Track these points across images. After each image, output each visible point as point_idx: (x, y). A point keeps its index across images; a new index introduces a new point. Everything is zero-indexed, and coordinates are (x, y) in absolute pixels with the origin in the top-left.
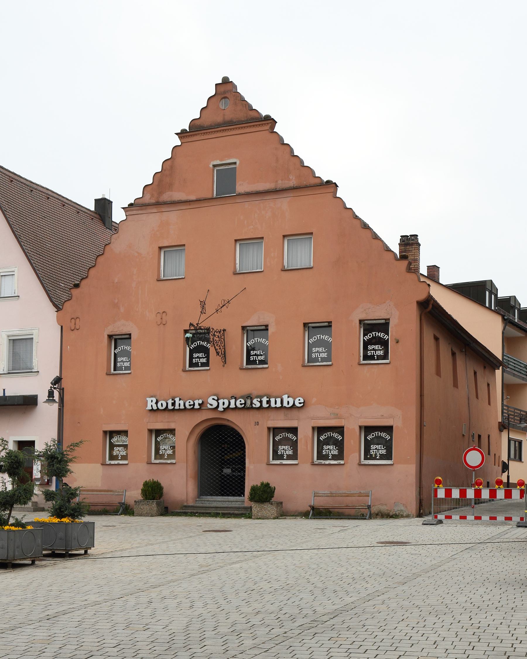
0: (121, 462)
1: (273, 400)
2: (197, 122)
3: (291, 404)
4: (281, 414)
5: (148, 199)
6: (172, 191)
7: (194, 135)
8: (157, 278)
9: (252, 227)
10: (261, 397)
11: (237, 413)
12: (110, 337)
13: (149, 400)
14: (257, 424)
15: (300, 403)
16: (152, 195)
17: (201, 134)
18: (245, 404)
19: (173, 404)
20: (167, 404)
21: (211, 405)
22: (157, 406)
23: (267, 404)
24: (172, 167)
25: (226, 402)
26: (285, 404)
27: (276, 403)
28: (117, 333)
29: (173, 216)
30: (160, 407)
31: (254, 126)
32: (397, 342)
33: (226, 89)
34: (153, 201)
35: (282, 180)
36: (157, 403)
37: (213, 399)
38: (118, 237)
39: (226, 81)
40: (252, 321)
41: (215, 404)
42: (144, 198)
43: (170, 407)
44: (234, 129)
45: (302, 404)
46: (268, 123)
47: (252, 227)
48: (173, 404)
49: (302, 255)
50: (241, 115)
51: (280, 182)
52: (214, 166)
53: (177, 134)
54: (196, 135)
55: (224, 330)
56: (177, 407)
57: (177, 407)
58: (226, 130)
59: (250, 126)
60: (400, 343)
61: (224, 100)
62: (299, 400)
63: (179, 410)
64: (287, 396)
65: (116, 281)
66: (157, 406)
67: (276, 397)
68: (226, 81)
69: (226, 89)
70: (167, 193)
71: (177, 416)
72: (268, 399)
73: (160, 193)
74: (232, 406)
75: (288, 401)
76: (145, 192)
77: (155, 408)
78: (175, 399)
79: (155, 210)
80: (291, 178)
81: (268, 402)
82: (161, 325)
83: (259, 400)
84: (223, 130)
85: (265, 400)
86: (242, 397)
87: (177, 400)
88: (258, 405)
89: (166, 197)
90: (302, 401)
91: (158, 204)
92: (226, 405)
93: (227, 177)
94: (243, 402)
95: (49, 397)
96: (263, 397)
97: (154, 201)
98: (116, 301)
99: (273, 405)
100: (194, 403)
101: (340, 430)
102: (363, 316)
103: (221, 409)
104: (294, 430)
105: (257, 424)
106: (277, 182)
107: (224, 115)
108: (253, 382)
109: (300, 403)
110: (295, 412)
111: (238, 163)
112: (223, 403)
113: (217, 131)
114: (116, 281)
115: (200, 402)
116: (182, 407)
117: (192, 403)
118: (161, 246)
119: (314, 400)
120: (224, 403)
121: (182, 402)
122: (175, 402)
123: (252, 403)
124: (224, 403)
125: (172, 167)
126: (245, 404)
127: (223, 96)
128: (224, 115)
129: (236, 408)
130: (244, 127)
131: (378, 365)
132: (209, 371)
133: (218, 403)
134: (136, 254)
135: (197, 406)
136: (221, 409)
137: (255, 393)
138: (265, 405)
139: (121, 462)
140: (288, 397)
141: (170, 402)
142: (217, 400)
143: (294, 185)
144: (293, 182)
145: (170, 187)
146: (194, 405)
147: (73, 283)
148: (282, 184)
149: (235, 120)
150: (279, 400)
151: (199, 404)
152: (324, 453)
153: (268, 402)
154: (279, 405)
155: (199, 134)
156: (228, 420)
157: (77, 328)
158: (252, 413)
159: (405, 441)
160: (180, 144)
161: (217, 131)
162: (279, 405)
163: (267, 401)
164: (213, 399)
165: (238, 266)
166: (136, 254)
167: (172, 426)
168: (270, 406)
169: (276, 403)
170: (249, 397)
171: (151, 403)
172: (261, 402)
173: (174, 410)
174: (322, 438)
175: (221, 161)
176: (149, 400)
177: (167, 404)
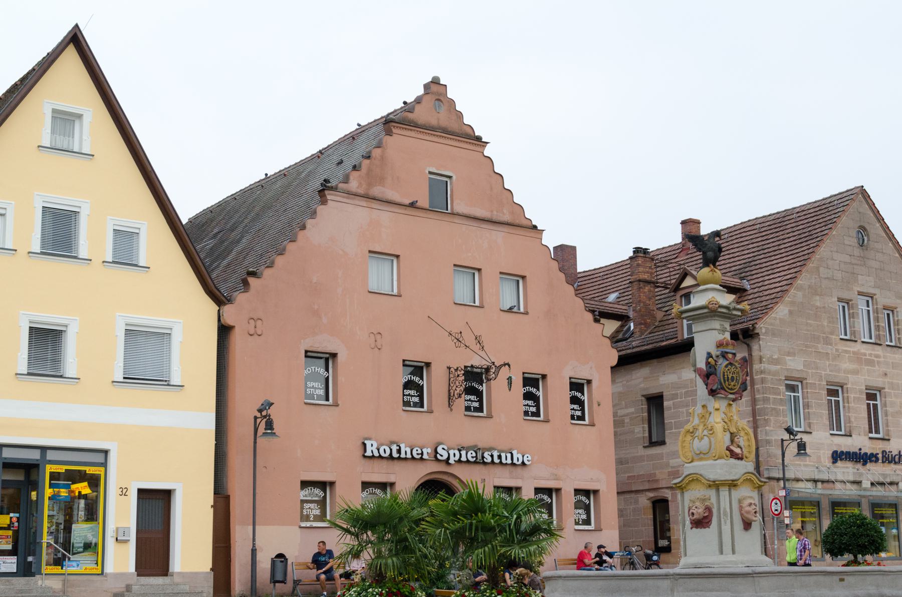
0: (315, 524)
6: (383, 186)
16: (360, 185)
18: (476, 457)
19: (399, 451)
20: (391, 450)
28: (319, 350)
33: (435, 88)
39: (435, 81)
43: (395, 455)
48: (399, 451)
52: (430, 173)
56: (403, 455)
57: (403, 455)
63: (406, 459)
65: (315, 280)
68: (435, 81)
69: (435, 88)
70: (379, 187)
71: (397, 465)
73: (370, 185)
74: (464, 459)
77: (376, 454)
79: (364, 204)
81: (500, 457)
85: (496, 454)
89: (376, 191)
90: (530, 458)
91: (367, 197)
92: (457, 458)
93: (440, 188)
98: (316, 307)
102: (572, 375)
108: (475, 432)
111: (454, 178)
114: (315, 280)
128: (438, 119)
129: (468, 461)
134: (341, 252)
138: (496, 460)
139: (315, 524)
144: (506, 218)
146: (422, 454)
148: (497, 216)
150: (509, 455)
153: (500, 457)
166: (341, 252)
167: (392, 479)
172: (492, 456)
173: (399, 458)
177: (391, 450)
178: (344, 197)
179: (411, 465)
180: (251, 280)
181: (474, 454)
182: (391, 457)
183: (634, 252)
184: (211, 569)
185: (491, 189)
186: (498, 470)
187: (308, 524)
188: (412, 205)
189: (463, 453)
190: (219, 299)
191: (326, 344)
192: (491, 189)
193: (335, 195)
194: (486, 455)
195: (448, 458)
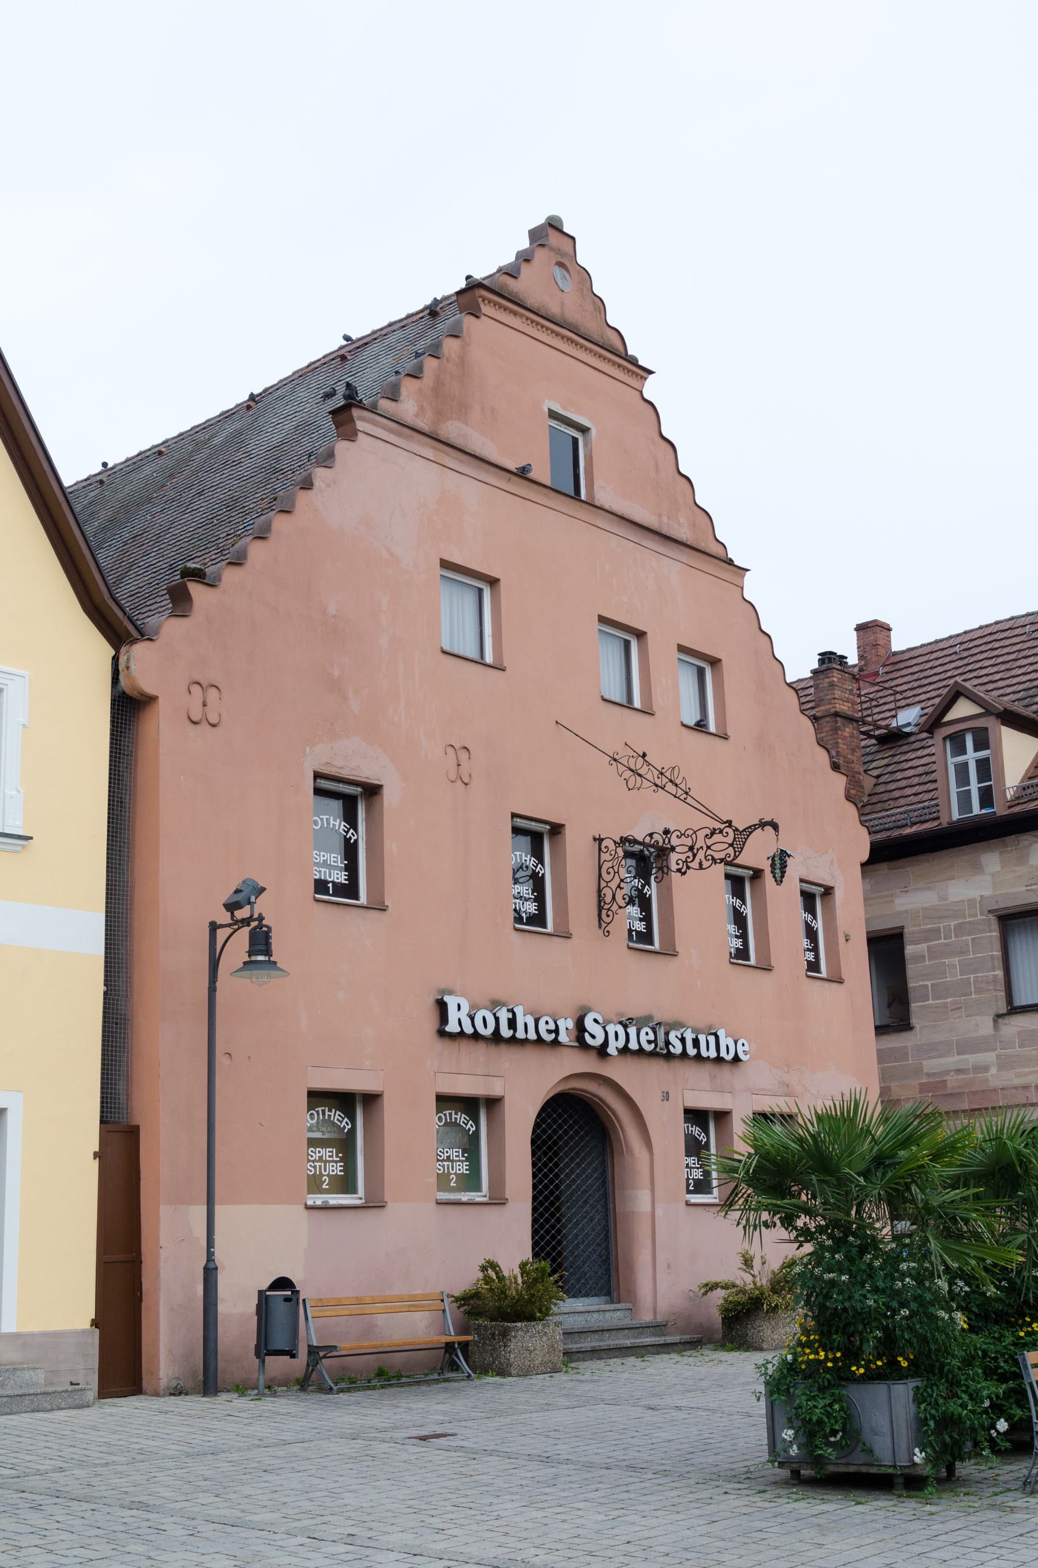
6: (466, 423)
17: (527, 319)
19: (512, 1024)
20: (497, 1019)
28: (345, 773)
30: (481, 1030)
31: (620, 366)
39: (554, 225)
43: (506, 1032)
44: (586, 349)
54: (515, 314)
57: (520, 1034)
58: (573, 341)
59: (614, 363)
63: (526, 1040)
68: (554, 225)
70: (457, 424)
71: (508, 1056)
73: (440, 415)
77: (469, 1030)
79: (429, 453)
82: (459, 783)
85: (689, 1036)
88: (677, 1049)
89: (452, 430)
90: (746, 1048)
92: (621, 1044)
100: (557, 1026)
105: (666, 1096)
111: (594, 432)
113: (557, 334)
114: (332, 610)
116: (532, 1036)
122: (514, 1014)
128: (562, 304)
129: (641, 1051)
130: (605, 358)
144: (683, 533)
146: (556, 1031)
150: (712, 1039)
153: (696, 1043)
155: (521, 316)
157: (213, 719)
161: (557, 334)
167: (495, 1089)
172: (683, 1040)
175: (564, 408)
177: (497, 1019)
178: (384, 428)
179: (531, 1057)
180: (195, 589)
181: (651, 1037)
182: (496, 1036)
183: (822, 662)
184: (95, 1323)
185: (657, 470)
187: (318, 1200)
188: (523, 473)
189: (632, 1031)
190: (117, 628)
191: (359, 762)
193: (375, 424)
194: (673, 1037)
195: (606, 1043)
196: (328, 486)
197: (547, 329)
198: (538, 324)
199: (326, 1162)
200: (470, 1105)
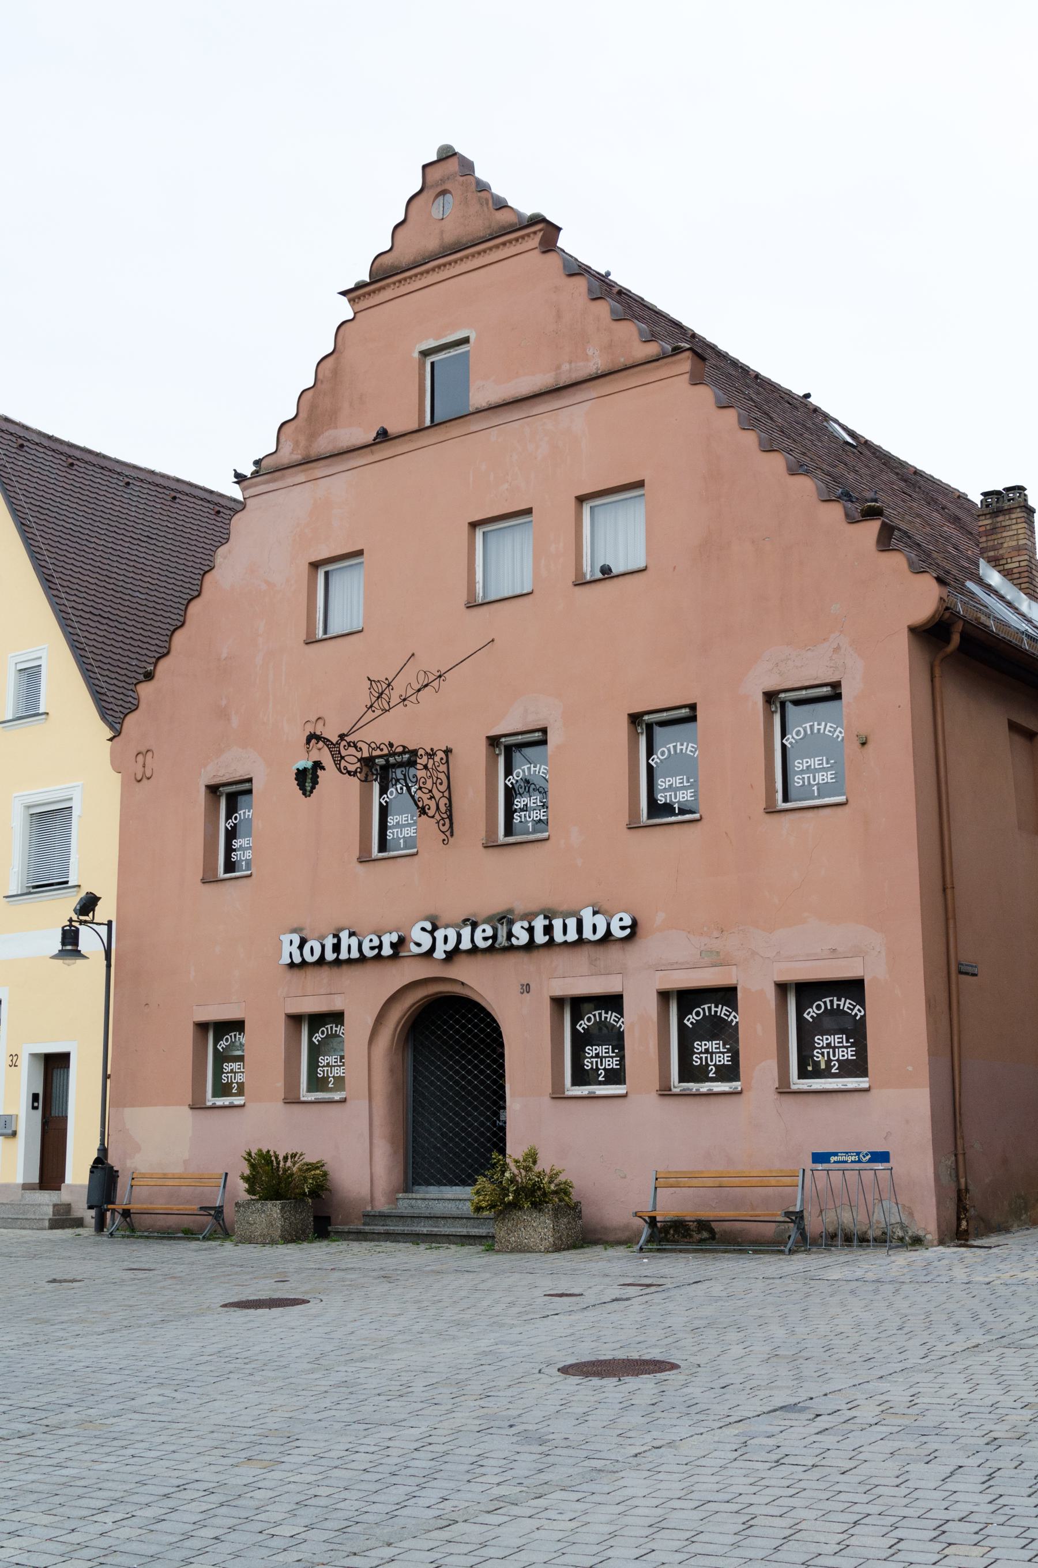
1: (558, 924)
2: (387, 260)
3: (601, 932)
4: (582, 958)
5: (287, 455)
7: (379, 289)
8: (304, 637)
9: (506, 486)
10: (530, 916)
11: (480, 960)
12: (213, 790)
13: (286, 938)
14: (526, 988)
15: (623, 928)
16: (297, 443)
17: (394, 283)
18: (494, 937)
19: (337, 948)
20: (323, 947)
21: (419, 945)
22: (302, 955)
23: (545, 935)
24: (335, 372)
25: (452, 933)
26: (588, 934)
27: (565, 932)
29: (338, 485)
30: (309, 958)
31: (504, 244)
32: (863, 744)
33: (447, 172)
34: (297, 457)
35: (570, 363)
36: (301, 947)
37: (423, 929)
38: (230, 552)
39: (447, 154)
40: (507, 725)
41: (426, 941)
42: (278, 453)
43: (330, 956)
44: (461, 259)
45: (628, 931)
46: (535, 233)
47: (506, 486)
48: (337, 948)
49: (621, 537)
50: (477, 224)
51: (566, 367)
52: (425, 354)
53: (344, 293)
54: (383, 288)
55: (448, 752)
56: (343, 955)
57: (343, 955)
58: (444, 265)
59: (497, 247)
60: (870, 746)
61: (441, 198)
62: (621, 919)
63: (350, 961)
64: (590, 910)
65: (224, 656)
66: (302, 955)
67: (566, 915)
68: (447, 154)
69: (447, 172)
70: (327, 434)
71: (348, 977)
72: (547, 922)
73: (312, 436)
75: (594, 925)
76: (282, 439)
78: (341, 935)
79: (301, 478)
80: (590, 352)
81: (548, 930)
83: (526, 925)
84: (439, 267)
85: (539, 923)
86: (487, 921)
87: (344, 935)
88: (523, 938)
89: (323, 444)
90: (628, 922)
91: (307, 462)
92: (450, 946)
94: (489, 932)
95: (63, 944)
96: (535, 915)
97: (299, 457)
98: (224, 703)
99: (559, 937)
100: (381, 942)
101: (727, 995)
102: (772, 683)
103: (439, 954)
104: (614, 1002)
105: (526, 988)
106: (558, 367)
107: (442, 232)
109: (623, 928)
110: (614, 953)
112: (446, 939)
113: (427, 272)
115: (394, 938)
116: (355, 954)
117: (376, 943)
118: (313, 559)
119: (660, 918)
120: (446, 938)
121: (354, 942)
122: (339, 940)
123: (510, 935)
124: (446, 938)
125: (335, 372)
126: (494, 937)
127: (439, 189)
129: (475, 950)
131: (816, 810)
132: (416, 858)
133: (434, 939)
135: (387, 951)
136: (439, 954)
137: (520, 908)
138: (540, 938)
140: (595, 913)
141: (329, 942)
142: (432, 933)
143: (598, 369)
145: (332, 418)
146: (380, 947)
147: (142, 671)
149: (464, 240)
150: (572, 923)
151: (393, 945)
152: (696, 1061)
153: (548, 930)
154: (572, 936)
155: (388, 285)
156: (463, 984)
158: (511, 961)
159: (899, 1019)
160: (351, 316)
161: (427, 272)
162: (572, 936)
163: (545, 926)
164: (423, 929)
165: (479, 587)
167: (336, 1004)
168: (552, 939)
169: (565, 932)
170: (506, 919)
171: (288, 949)
172: (531, 930)
173: (337, 962)
174: (690, 1020)
175: (436, 339)
176: (286, 938)
177: (323, 947)
182: (321, 961)
185: (559, 316)
186: (559, 960)
188: (383, 436)
189: (466, 932)
192: (559, 316)
195: (433, 948)
196: (225, 558)
197: (410, 277)
198: (405, 279)
199: (834, 1048)
200: (317, 1020)
